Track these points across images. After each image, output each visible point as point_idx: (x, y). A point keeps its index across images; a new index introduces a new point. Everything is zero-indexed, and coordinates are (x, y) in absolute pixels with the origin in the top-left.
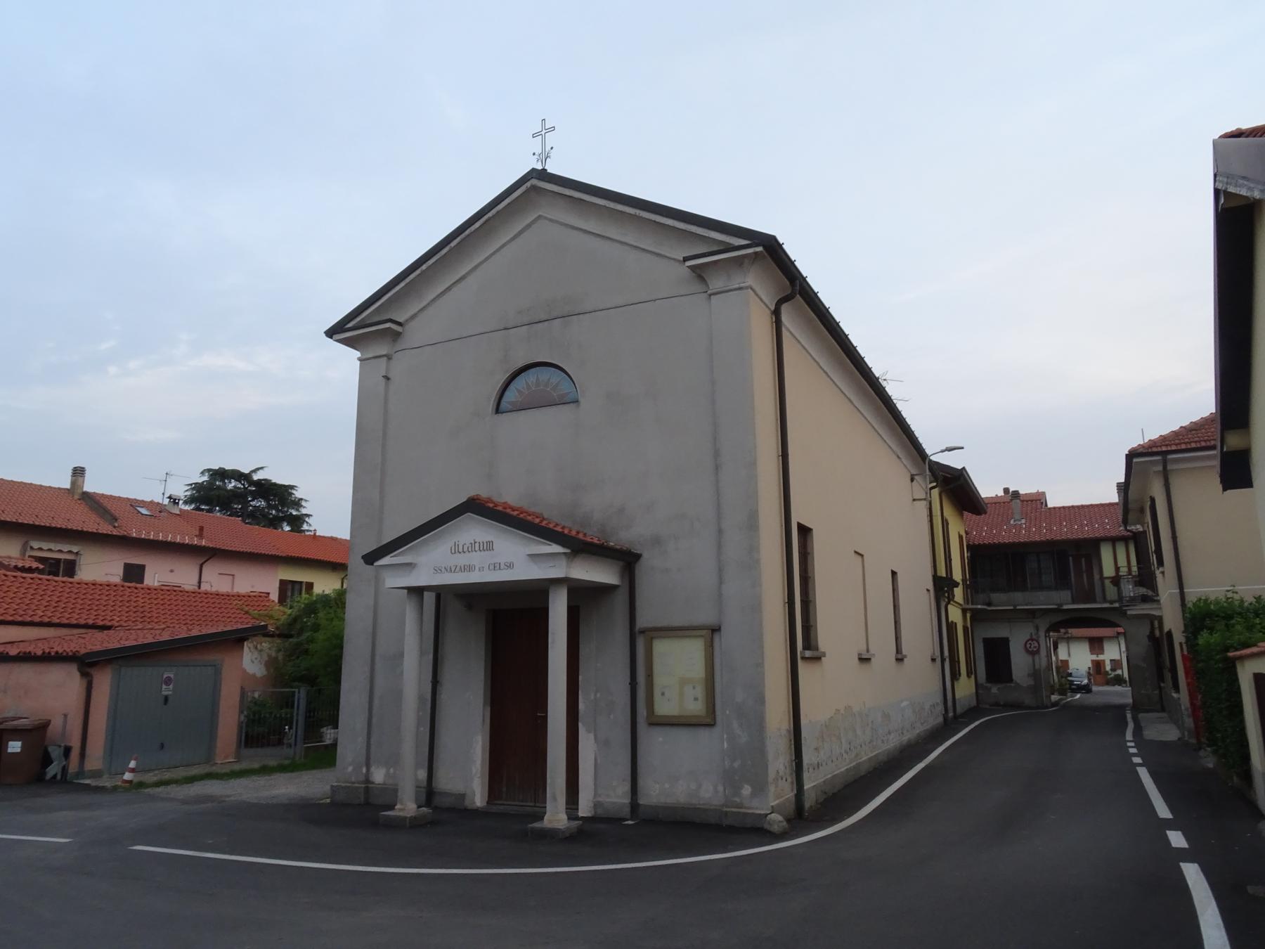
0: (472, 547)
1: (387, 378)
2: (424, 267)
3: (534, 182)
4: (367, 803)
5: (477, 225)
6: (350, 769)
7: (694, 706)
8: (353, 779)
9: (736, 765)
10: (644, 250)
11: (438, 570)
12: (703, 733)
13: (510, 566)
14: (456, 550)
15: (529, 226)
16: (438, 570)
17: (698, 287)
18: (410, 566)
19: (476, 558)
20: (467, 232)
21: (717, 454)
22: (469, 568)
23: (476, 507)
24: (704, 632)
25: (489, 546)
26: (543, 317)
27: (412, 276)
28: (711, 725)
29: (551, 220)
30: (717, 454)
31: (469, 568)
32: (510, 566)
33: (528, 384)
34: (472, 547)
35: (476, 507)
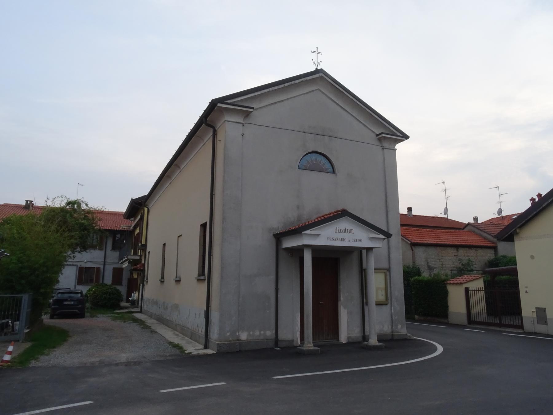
0: (344, 231)
1: (243, 135)
2: (271, 89)
3: (323, 75)
4: (240, 351)
5: (297, 81)
6: (228, 334)
7: (382, 298)
8: (230, 339)
9: (396, 318)
10: (360, 122)
11: (329, 239)
12: (384, 307)
13: (360, 241)
14: (337, 231)
15: (313, 91)
16: (329, 239)
17: (377, 143)
18: (318, 235)
19: (346, 236)
20: (293, 82)
21: (387, 207)
22: (344, 240)
23: (343, 214)
24: (385, 271)
25: (352, 232)
26: (321, 133)
27: (265, 91)
28: (386, 304)
29: (323, 93)
30: (387, 207)
31: (344, 240)
32: (360, 241)
33: (319, 161)
34: (344, 231)
35: (343, 214)
